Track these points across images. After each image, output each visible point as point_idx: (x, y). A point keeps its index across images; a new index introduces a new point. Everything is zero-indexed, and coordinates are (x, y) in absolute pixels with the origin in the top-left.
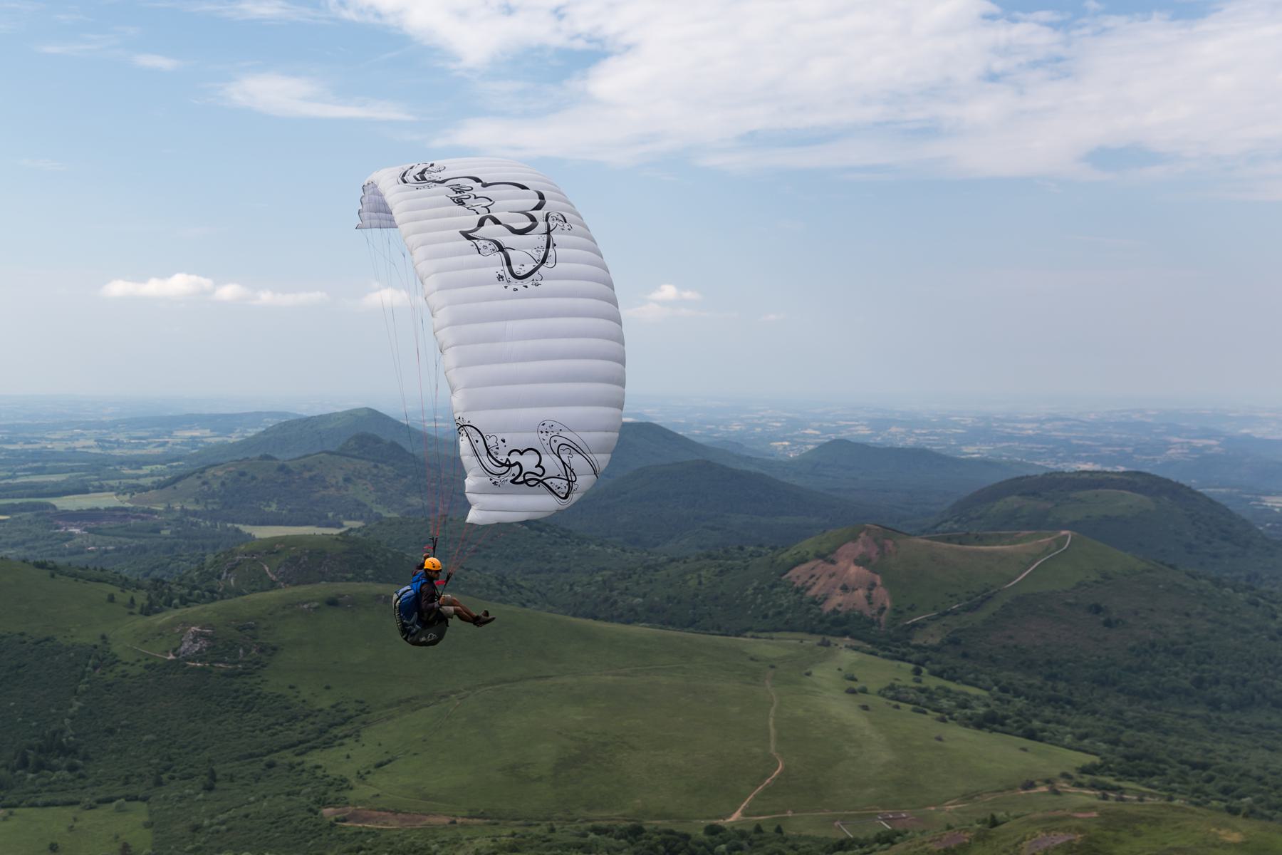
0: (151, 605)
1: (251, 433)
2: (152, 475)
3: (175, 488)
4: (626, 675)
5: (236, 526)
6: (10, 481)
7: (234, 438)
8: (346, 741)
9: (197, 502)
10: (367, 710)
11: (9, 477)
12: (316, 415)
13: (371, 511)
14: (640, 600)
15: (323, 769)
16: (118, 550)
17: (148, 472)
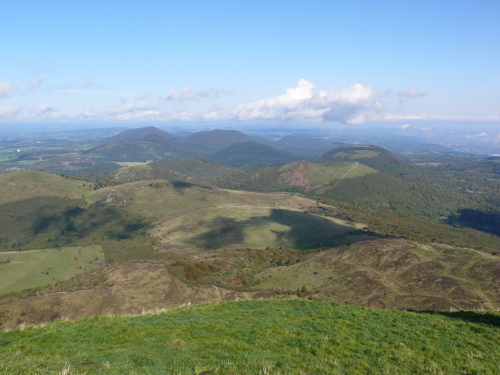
0: (96, 187)
1: (116, 133)
2: (87, 146)
3: (95, 151)
4: (238, 205)
5: (114, 162)
6: (45, 149)
7: (111, 136)
8: (158, 226)
9: (102, 155)
10: (163, 217)
11: (44, 148)
12: (136, 128)
13: (154, 157)
14: (239, 183)
15: (152, 234)
16: (80, 170)
17: (86, 146)
